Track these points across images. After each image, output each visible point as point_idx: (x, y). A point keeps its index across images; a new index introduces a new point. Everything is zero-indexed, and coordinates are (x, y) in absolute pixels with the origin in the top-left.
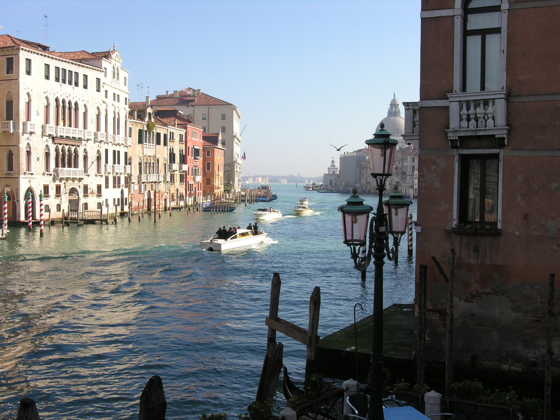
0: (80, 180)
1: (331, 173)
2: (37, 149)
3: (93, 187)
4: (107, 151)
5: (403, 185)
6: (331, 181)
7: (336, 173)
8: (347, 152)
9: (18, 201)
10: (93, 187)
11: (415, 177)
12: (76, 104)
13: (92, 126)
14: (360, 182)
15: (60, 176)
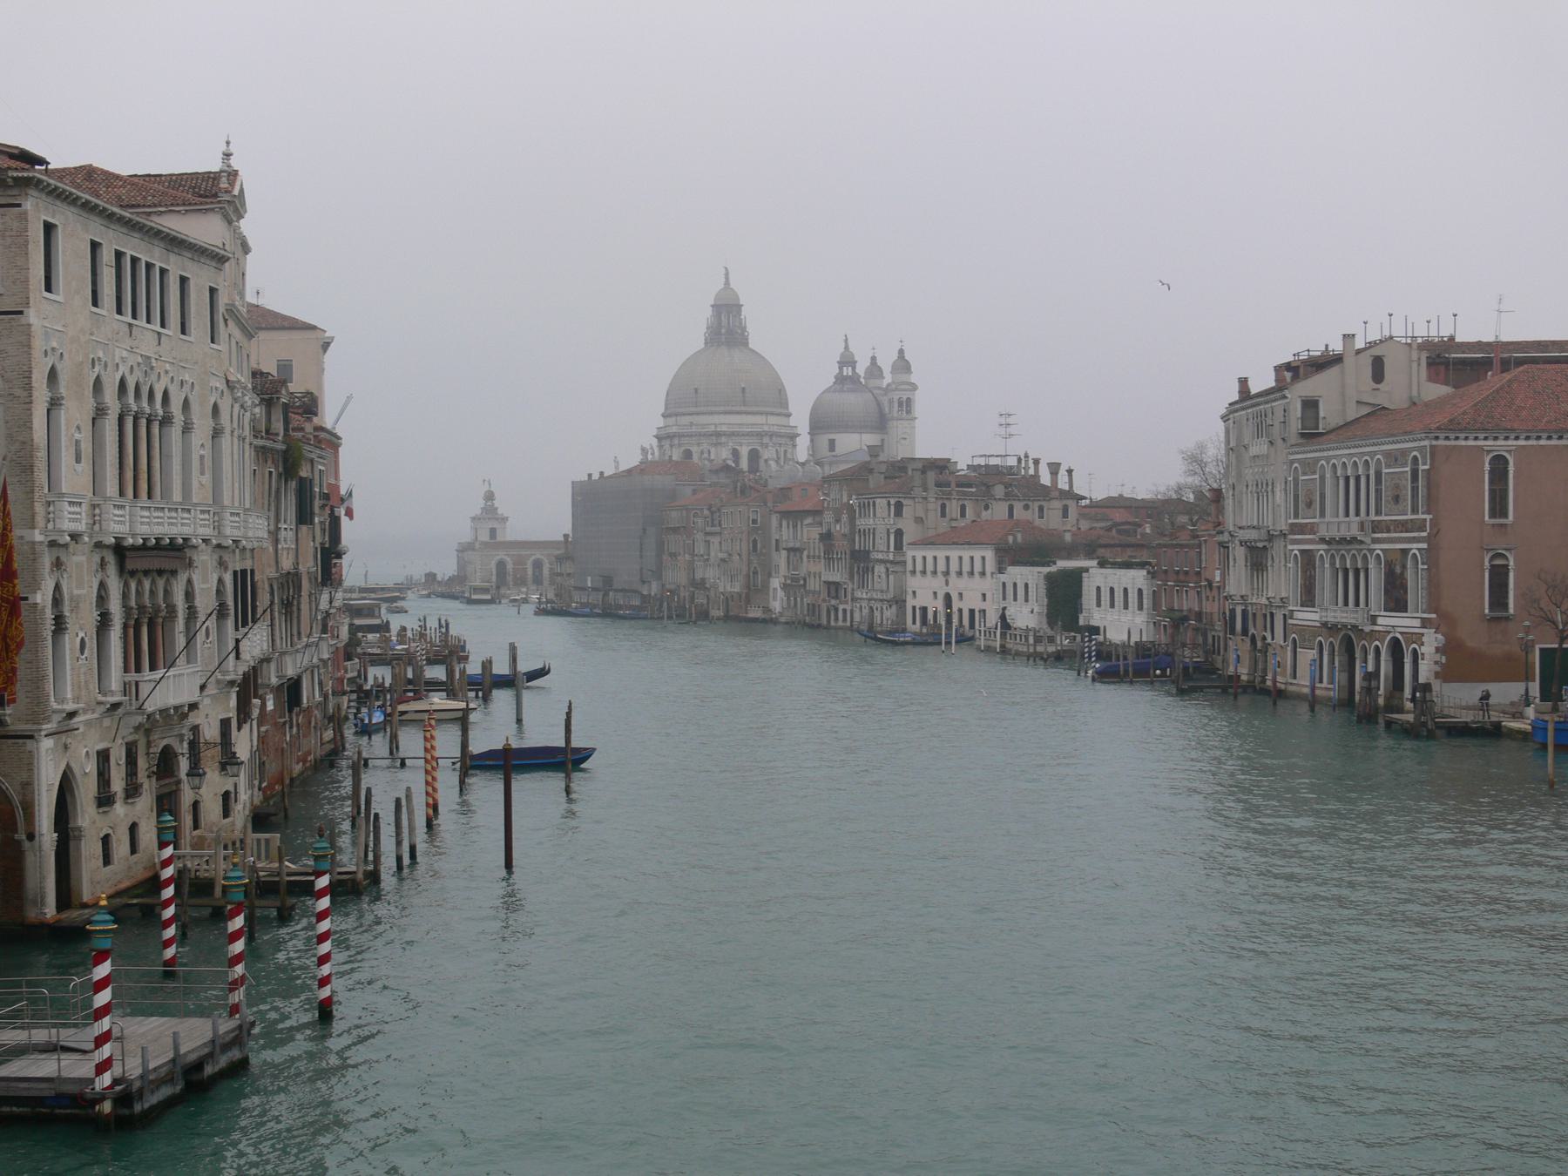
0: (193, 706)
1: (484, 537)
2: (77, 607)
3: (211, 732)
4: (235, 573)
5: (858, 594)
6: (501, 565)
7: (499, 539)
8: (602, 473)
9: (31, 837)
10: (211, 732)
11: (910, 567)
12: (166, 394)
13: (201, 483)
14: (659, 577)
15: (150, 710)
